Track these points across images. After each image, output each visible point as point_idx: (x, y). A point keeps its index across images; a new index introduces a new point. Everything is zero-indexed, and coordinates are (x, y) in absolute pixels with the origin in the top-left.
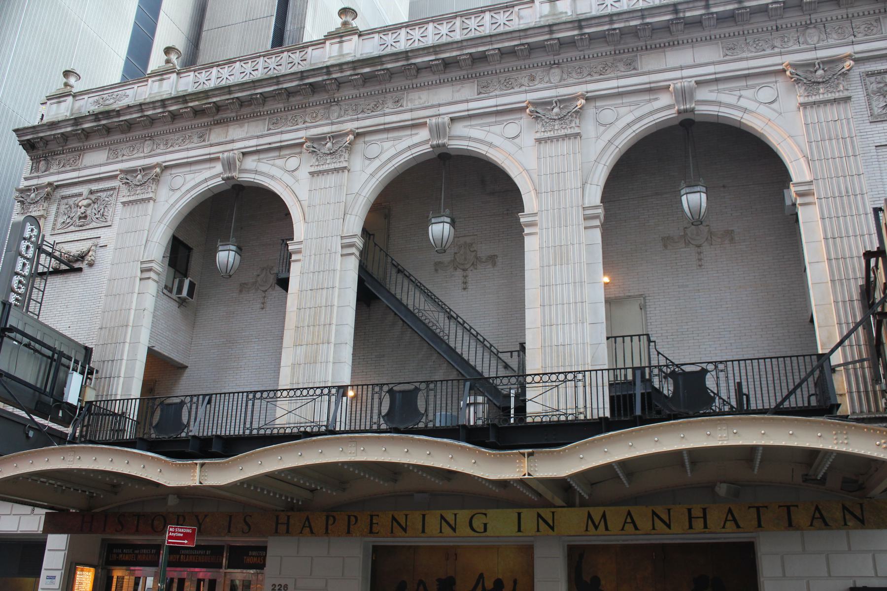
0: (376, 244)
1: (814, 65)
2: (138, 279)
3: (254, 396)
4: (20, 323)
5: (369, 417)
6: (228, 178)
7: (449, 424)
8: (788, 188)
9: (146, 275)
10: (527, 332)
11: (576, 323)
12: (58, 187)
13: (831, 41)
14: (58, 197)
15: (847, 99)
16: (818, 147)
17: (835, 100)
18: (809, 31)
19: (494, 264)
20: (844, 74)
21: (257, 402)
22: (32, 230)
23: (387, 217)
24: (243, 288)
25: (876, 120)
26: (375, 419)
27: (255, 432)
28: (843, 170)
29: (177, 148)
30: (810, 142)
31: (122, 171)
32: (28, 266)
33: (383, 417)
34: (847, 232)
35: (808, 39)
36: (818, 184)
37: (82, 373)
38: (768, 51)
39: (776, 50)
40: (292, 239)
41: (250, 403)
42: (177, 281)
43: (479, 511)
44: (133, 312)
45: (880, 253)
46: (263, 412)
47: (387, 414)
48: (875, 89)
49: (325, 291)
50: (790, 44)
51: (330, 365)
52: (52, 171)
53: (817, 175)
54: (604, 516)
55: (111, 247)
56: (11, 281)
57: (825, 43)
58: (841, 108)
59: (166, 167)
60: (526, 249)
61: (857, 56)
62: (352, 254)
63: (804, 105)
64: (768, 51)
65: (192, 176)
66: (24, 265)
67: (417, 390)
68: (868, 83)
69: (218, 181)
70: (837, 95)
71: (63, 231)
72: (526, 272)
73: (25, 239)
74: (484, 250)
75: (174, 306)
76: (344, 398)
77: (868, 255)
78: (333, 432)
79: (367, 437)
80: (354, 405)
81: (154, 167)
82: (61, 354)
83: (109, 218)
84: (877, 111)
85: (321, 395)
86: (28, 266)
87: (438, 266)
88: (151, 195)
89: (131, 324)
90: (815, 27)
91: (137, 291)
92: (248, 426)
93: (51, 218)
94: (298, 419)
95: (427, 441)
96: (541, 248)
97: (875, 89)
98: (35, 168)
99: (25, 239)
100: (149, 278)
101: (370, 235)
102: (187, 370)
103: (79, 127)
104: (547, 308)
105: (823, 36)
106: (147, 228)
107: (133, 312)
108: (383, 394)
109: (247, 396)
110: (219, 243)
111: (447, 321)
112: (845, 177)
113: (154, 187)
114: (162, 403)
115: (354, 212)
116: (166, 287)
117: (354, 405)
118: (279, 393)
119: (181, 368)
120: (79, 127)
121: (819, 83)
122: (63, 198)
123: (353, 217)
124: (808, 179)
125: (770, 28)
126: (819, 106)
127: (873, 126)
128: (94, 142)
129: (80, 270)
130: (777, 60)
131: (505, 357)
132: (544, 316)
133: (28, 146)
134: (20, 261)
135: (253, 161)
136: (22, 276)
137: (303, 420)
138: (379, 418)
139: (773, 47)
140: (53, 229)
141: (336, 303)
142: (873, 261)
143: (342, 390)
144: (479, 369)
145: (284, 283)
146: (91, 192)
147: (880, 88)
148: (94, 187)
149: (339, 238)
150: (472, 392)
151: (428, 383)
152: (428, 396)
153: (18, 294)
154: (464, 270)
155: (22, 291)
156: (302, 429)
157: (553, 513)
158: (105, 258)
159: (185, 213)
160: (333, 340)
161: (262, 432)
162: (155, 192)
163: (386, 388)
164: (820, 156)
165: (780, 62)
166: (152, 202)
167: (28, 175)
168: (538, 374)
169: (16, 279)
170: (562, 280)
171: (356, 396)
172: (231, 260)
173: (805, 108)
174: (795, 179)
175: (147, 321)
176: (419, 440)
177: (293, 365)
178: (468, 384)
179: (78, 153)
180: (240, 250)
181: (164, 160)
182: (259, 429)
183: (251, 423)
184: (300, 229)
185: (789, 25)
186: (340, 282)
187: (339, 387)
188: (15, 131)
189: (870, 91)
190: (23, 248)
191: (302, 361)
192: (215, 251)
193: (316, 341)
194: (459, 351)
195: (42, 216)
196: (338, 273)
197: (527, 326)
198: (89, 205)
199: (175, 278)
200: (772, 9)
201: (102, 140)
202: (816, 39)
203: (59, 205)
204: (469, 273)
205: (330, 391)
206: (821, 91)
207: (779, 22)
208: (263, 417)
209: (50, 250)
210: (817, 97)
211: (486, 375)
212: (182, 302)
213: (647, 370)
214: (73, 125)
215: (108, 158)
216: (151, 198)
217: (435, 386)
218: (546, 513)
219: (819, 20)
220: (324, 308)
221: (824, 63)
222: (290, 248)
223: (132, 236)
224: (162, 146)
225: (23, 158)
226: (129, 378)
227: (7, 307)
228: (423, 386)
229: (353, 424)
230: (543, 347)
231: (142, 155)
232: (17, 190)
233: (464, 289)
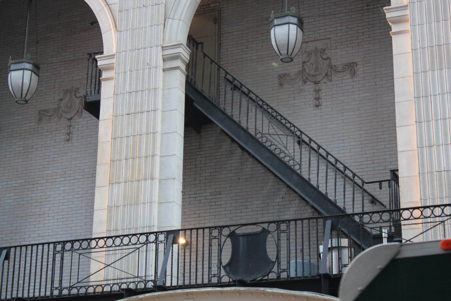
0: (205, 55)
3: (63, 248)
5: (206, 269)
7: (307, 274)
10: (400, 156)
19: (353, 74)
21: (67, 255)
23: (217, 20)
24: (43, 115)
26: (215, 270)
27: (65, 292)
33: (224, 267)
40: (102, 53)
41: (58, 256)
46: (75, 268)
47: (229, 264)
49: (145, 115)
51: (156, 207)
60: (394, 53)
62: (177, 68)
67: (265, 232)
72: (396, 81)
74: (339, 57)
76: (175, 246)
78: (163, 288)
79: (208, 292)
80: (188, 254)
85: (147, 243)
87: (283, 79)
92: (56, 285)
94: (118, 274)
95: (282, 295)
96: (414, 50)
101: (198, 44)
104: (424, 125)
108: (223, 239)
109: (55, 248)
110: (11, 62)
111: (297, 147)
115: (177, 16)
117: (188, 254)
118: (93, 243)
123: (176, 22)
131: (373, 189)
132: (421, 135)
137: (124, 275)
138: (219, 268)
141: (159, 129)
143: (172, 235)
144: (340, 204)
145: (94, 108)
149: (160, 48)
150: (334, 233)
151: (278, 223)
152: (279, 239)
154: (316, 83)
156: (124, 286)
160: (157, 174)
161: (74, 291)
163: (226, 232)
168: (418, 208)
170: (442, 89)
171: (188, 245)
176: (273, 294)
177: (110, 208)
178: (329, 223)
180: (36, 69)
182: (71, 288)
183: (61, 281)
184: (110, 40)
187: (168, 233)
191: (121, 203)
192: (6, 71)
193: (136, 177)
194: (314, 182)
196: (160, 92)
197: (400, 148)
204: (322, 86)
205: (157, 238)
208: (74, 274)
211: (349, 211)
217: (288, 227)
220: (144, 136)
222: (99, 63)
228: (272, 227)
230: (421, 174)
233: (317, 106)
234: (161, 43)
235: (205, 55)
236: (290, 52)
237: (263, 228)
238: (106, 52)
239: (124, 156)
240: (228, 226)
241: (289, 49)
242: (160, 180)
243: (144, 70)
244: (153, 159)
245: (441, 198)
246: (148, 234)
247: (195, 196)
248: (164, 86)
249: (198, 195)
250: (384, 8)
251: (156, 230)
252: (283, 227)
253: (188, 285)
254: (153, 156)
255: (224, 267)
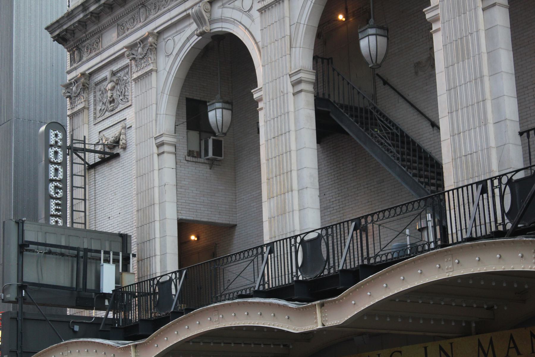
2: (156, 156)
4: (40, 234)
5: (360, 255)
6: (202, 34)
9: (161, 150)
11: (480, 127)
12: (91, 74)
14: (93, 85)
22: (56, 135)
29: (163, 10)
31: (126, 47)
32: (61, 170)
37: (116, 261)
42: (203, 143)
43: (396, 349)
44: (156, 190)
52: (84, 59)
54: (491, 343)
55: (133, 126)
56: (47, 189)
59: (159, 33)
65: (179, 36)
66: (56, 170)
69: (195, 39)
71: (101, 119)
73: (51, 146)
75: (203, 170)
81: (146, 38)
82: (86, 251)
83: (130, 99)
86: (61, 170)
88: (150, 67)
89: (157, 201)
91: (156, 167)
93: (92, 107)
98: (73, 60)
99: (51, 146)
100: (163, 153)
102: (237, 228)
103: (88, 12)
104: (454, 113)
106: (154, 101)
107: (156, 190)
113: (152, 56)
114: (158, 281)
115: (298, 45)
116: (190, 153)
119: (232, 227)
120: (88, 12)
122: (97, 84)
123: (298, 49)
128: (106, 20)
129: (118, 155)
132: (453, 124)
133: (60, 40)
134: (52, 168)
135: (219, 7)
136: (56, 181)
140: (95, 118)
146: (114, 74)
148: (115, 67)
153: (57, 199)
155: (60, 194)
157: (451, 344)
158: (132, 138)
159: (183, 76)
162: (156, 62)
166: (154, 74)
167: (69, 68)
169: (51, 186)
172: (219, 118)
175: (171, 195)
177: (270, 218)
179: (97, 36)
181: (154, 27)
186: (295, 124)
188: (47, 28)
190: (51, 155)
195: (84, 108)
198: (113, 88)
199: (201, 140)
201: (109, 18)
203: (95, 92)
209: (82, 146)
212: (212, 163)
213: (489, 182)
214: (83, 12)
215: (118, 35)
216: (151, 71)
218: (446, 345)
223: (149, 111)
224: (152, 11)
225: (62, 53)
226: (163, 254)
227: (21, 225)
229: (352, 263)
231: (141, 24)
232: (64, 86)
234: (288, 71)
235: (334, 70)
236: (374, 61)
237: (319, 234)
238: (259, 87)
239: (274, 175)
240: (299, 235)
241: (373, 58)
242: (299, 191)
243: (280, 97)
244: (291, 174)
245: (484, 174)
246: (257, 248)
247: (366, 186)
248: (295, 108)
249: (369, 185)
250: (424, 10)
251: (497, 174)
252: (330, 230)
253: (484, 236)
254: (291, 171)
255: (507, 214)
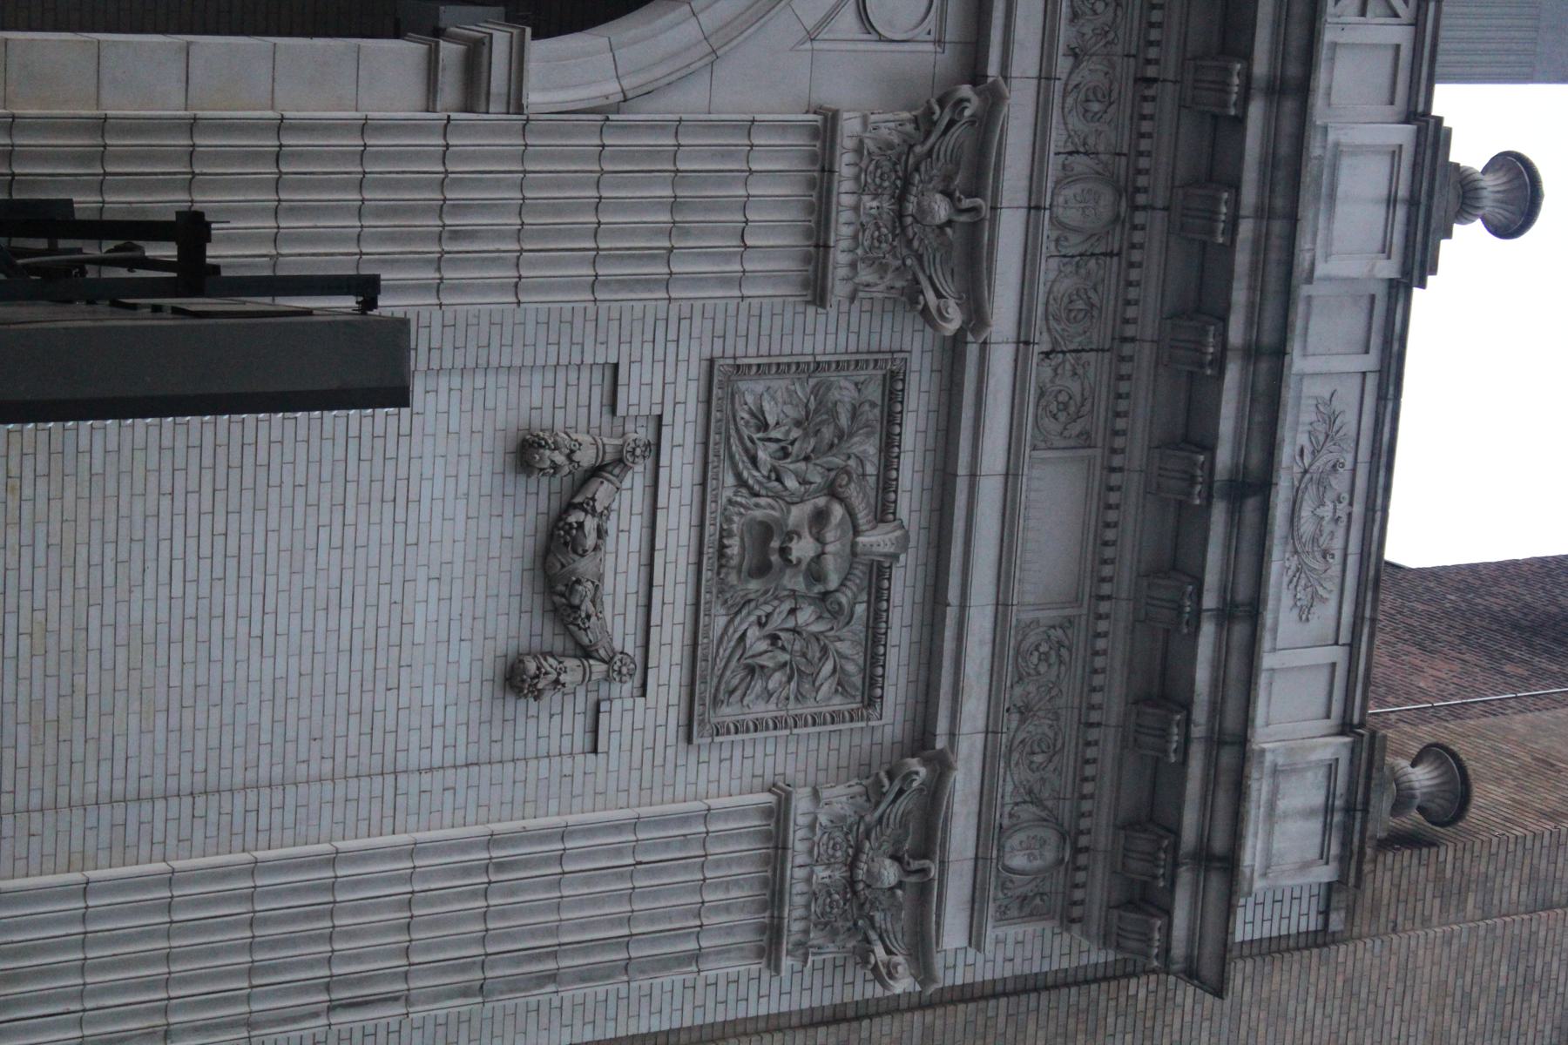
1: (974, 192)
8: (510, 19)
13: (1048, 269)
15: (816, 291)
16: (652, 154)
17: (823, 246)
18: (1107, 197)
20: (912, 294)
25: (720, 380)
28: (543, 234)
30: (678, 127)
34: (294, 211)
35: (1077, 188)
36: (506, 131)
38: (1065, 34)
39: (1063, 65)
45: (195, 273)
48: (835, 395)
50: (1075, 122)
53: (542, 133)
57: (1047, 247)
58: (784, 265)
61: (972, 351)
63: (826, 127)
64: (1065, 34)
68: (862, 375)
70: (840, 257)
77: (192, 230)
84: (750, 390)
90: (1116, 218)
97: (835, 395)
105: (1074, 245)
112: (518, 236)
121: (901, 199)
124: (535, 98)
125: (1153, 53)
126: (812, 184)
127: (696, 369)
130: (1026, 61)
139: (1076, 54)
142: (167, 251)
147: (834, 415)
164: (615, 157)
165: (1015, 71)
173: (815, 133)
174: (539, 50)
185: (1146, 126)
189: (832, 376)
200: (1227, 71)
202: (1071, 216)
206: (869, 202)
207: (1168, 94)
210: (847, 186)
219: (1138, 237)
221: (974, 229)
